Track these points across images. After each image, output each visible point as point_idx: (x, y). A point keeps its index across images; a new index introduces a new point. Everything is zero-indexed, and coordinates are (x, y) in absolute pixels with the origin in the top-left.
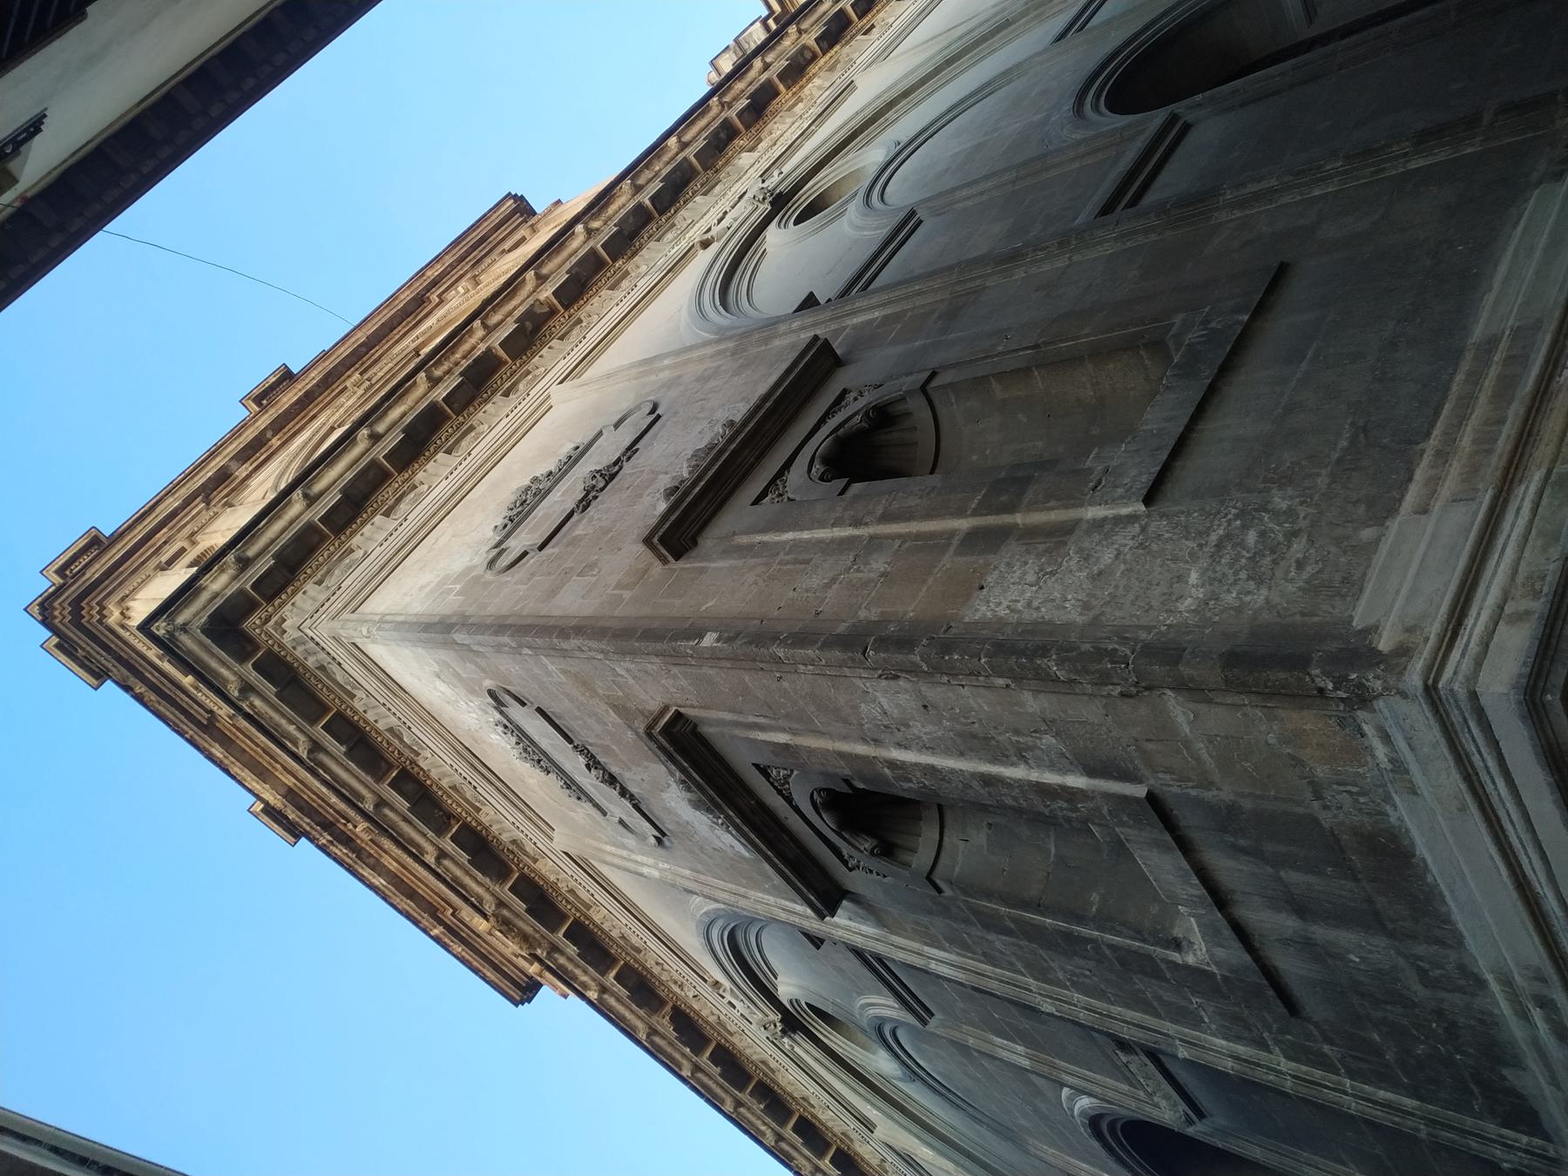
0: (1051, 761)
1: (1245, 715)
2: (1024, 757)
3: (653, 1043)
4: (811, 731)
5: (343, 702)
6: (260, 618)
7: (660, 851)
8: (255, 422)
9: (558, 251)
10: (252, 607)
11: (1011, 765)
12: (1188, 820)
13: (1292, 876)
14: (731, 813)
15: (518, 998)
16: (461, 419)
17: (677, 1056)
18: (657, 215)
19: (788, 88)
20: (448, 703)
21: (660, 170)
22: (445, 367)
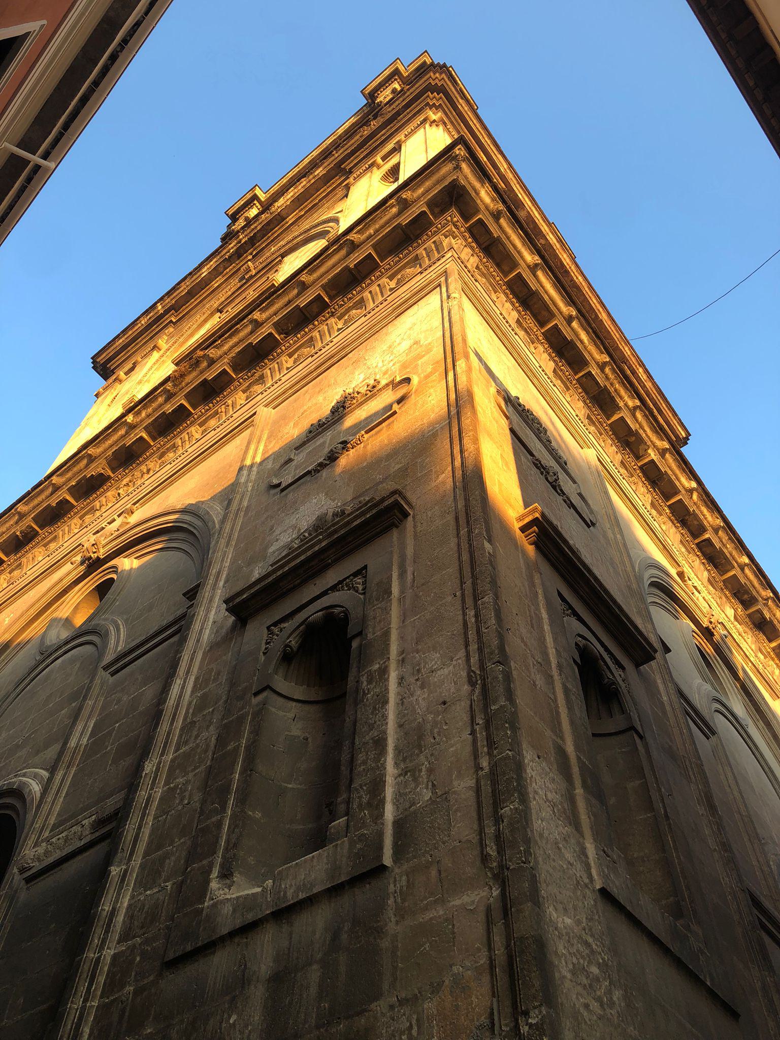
0: (406, 794)
1: (479, 950)
2: (406, 774)
3: (82, 458)
4: (404, 614)
5: (387, 270)
6: (458, 221)
7: (263, 487)
9: (680, 467)
10: (466, 217)
11: (396, 763)
12: (363, 895)
13: (314, 974)
14: (323, 544)
15: (98, 360)
16: (574, 382)
17: (69, 475)
18: (697, 541)
19: (774, 649)
20: (390, 347)
21: (727, 548)
22: (611, 376)
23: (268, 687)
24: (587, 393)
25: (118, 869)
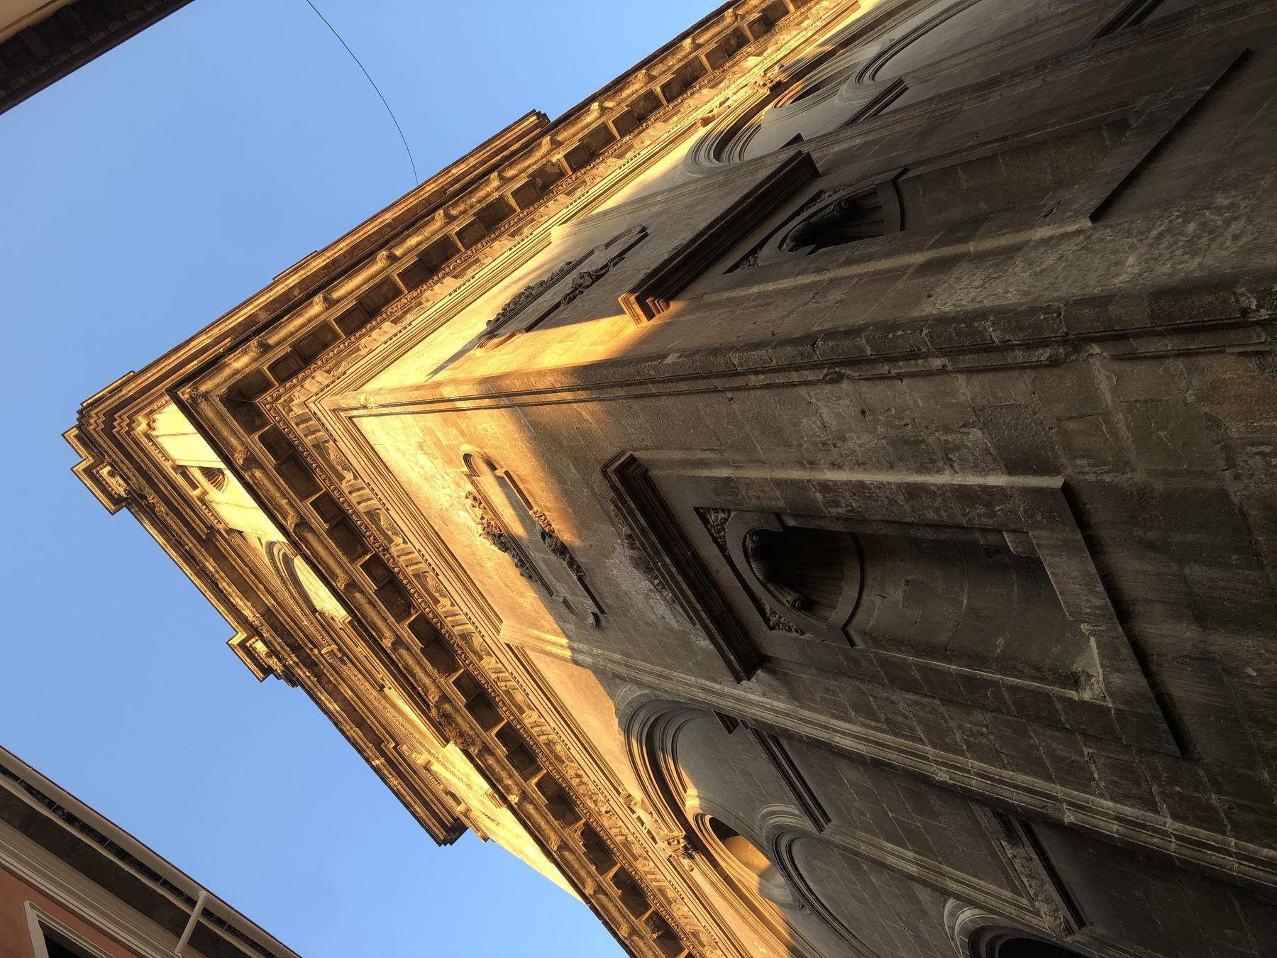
0: (975, 460)
1: (1166, 370)
2: (950, 460)
4: (754, 462)
5: (332, 483)
6: (272, 396)
7: (597, 635)
8: (286, 280)
9: (573, 123)
10: (267, 386)
11: (937, 472)
12: (1099, 513)
13: (1196, 572)
14: (668, 561)
15: (442, 838)
16: (469, 252)
17: (583, 873)
18: (665, 102)
19: (797, 8)
20: (426, 479)
21: (673, 65)
22: (462, 207)
23: (844, 629)
24: (482, 237)
25: (1068, 813)
